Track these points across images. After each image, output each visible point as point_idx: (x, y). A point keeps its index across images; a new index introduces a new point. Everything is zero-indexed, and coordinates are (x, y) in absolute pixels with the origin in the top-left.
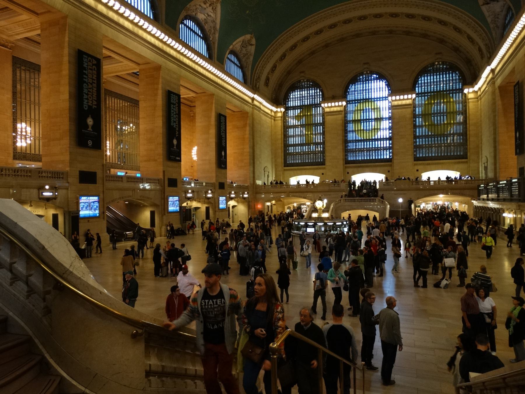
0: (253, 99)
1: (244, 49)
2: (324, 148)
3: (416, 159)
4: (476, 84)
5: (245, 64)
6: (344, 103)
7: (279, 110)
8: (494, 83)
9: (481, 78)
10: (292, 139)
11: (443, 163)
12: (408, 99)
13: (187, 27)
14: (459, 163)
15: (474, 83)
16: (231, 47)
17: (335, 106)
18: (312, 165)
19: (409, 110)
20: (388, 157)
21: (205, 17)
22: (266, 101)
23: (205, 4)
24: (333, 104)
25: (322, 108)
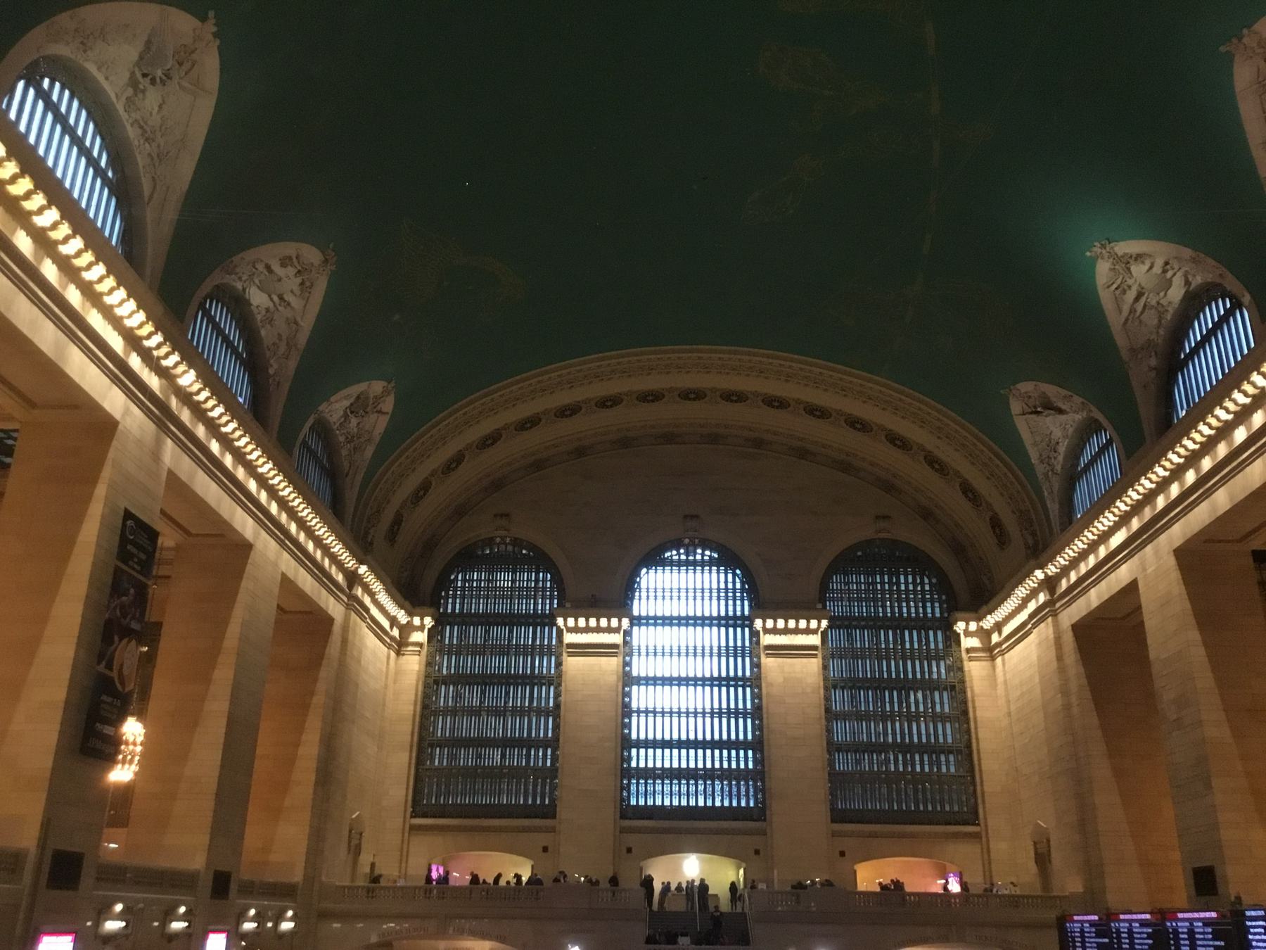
0: (353, 578)
1: (354, 421)
2: (555, 759)
5: (346, 464)
6: (625, 622)
7: (417, 621)
8: (1055, 614)
11: (913, 836)
12: (808, 631)
13: (211, 320)
14: (956, 836)
15: (985, 608)
16: (320, 408)
17: (598, 630)
18: (510, 816)
19: (813, 666)
21: (271, 305)
22: (388, 591)
23: (283, 265)
24: (593, 622)
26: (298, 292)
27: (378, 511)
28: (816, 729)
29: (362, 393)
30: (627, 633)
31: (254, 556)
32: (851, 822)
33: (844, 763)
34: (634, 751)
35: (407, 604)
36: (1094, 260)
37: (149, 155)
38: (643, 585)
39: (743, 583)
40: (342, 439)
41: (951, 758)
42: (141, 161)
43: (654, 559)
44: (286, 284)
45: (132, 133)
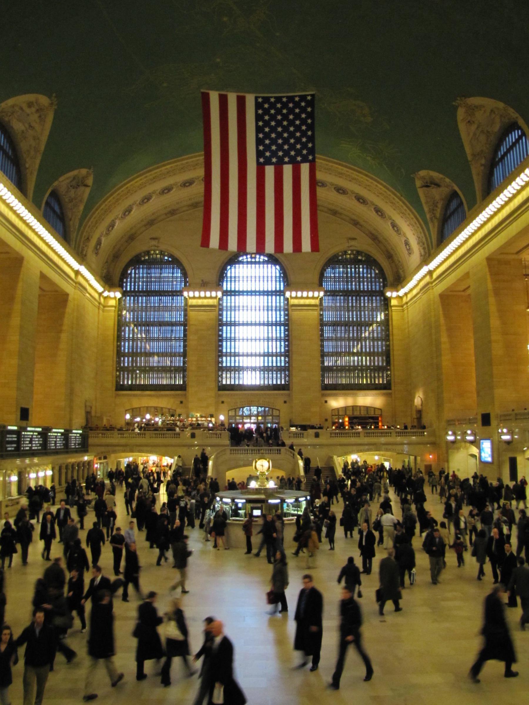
0: (77, 273)
1: (73, 191)
2: (184, 363)
3: (326, 387)
4: (403, 287)
7: (112, 294)
9: (411, 279)
10: (274, 351)
12: (313, 298)
15: (400, 287)
16: (56, 183)
17: (205, 298)
19: (315, 314)
20: (283, 382)
22: (96, 279)
25: (185, 298)
27: (88, 238)
28: (316, 347)
30: (221, 299)
31: (25, 263)
32: (330, 390)
33: (329, 362)
34: (224, 358)
36: (456, 108)
38: (229, 275)
39: (280, 274)
40: (67, 200)
41: (380, 358)
43: (233, 260)
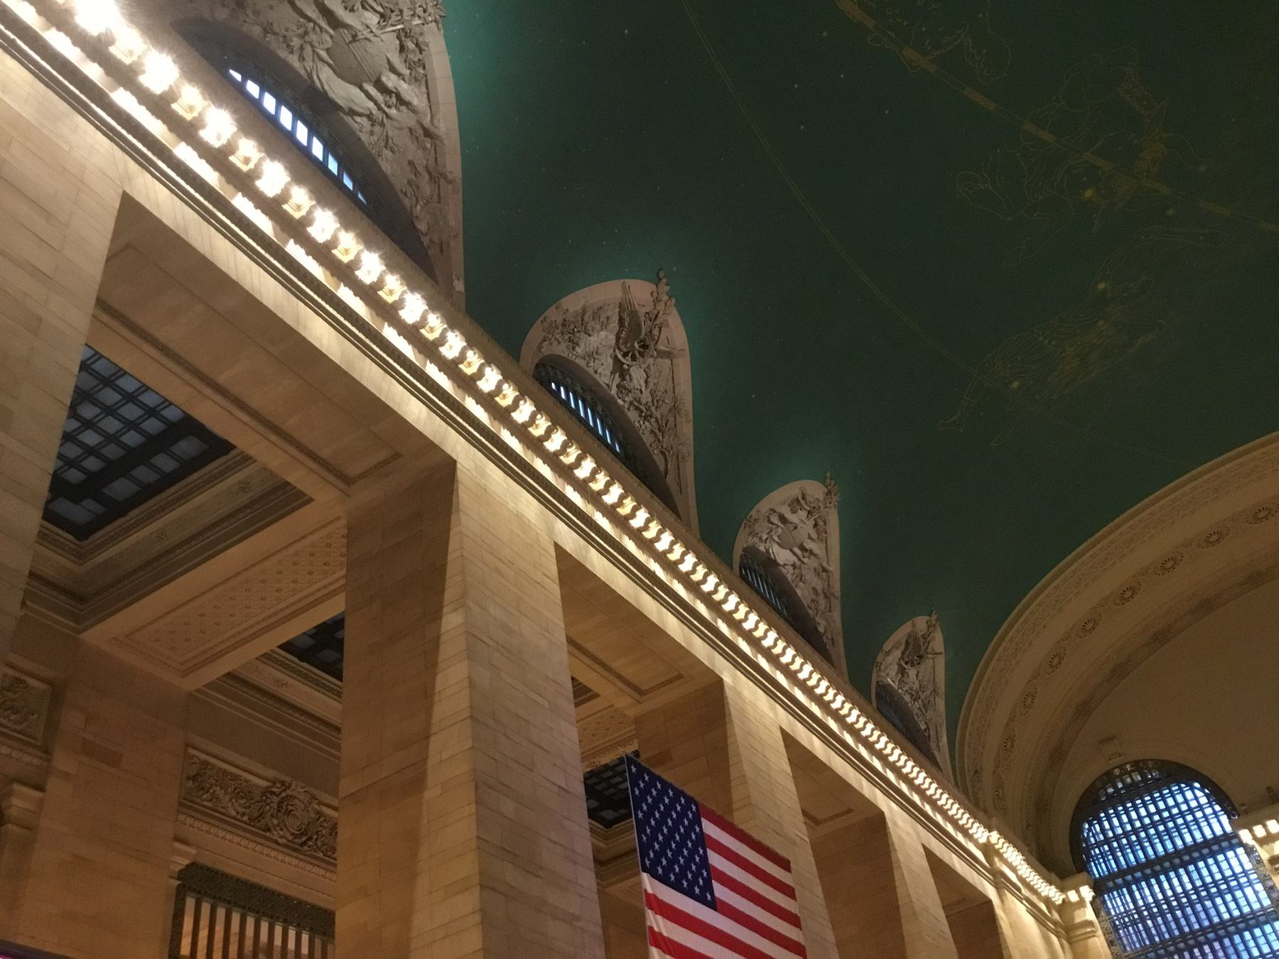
0: (988, 849)
1: (912, 672)
5: (923, 727)
7: (1073, 896)
21: (795, 559)
23: (794, 512)
26: (814, 536)
27: (976, 772)
29: (909, 635)
31: (890, 824)
35: (1053, 876)
37: (652, 432)
40: (907, 698)
42: (648, 439)
44: (802, 523)
45: (633, 415)
